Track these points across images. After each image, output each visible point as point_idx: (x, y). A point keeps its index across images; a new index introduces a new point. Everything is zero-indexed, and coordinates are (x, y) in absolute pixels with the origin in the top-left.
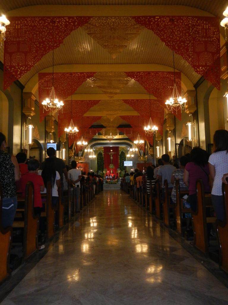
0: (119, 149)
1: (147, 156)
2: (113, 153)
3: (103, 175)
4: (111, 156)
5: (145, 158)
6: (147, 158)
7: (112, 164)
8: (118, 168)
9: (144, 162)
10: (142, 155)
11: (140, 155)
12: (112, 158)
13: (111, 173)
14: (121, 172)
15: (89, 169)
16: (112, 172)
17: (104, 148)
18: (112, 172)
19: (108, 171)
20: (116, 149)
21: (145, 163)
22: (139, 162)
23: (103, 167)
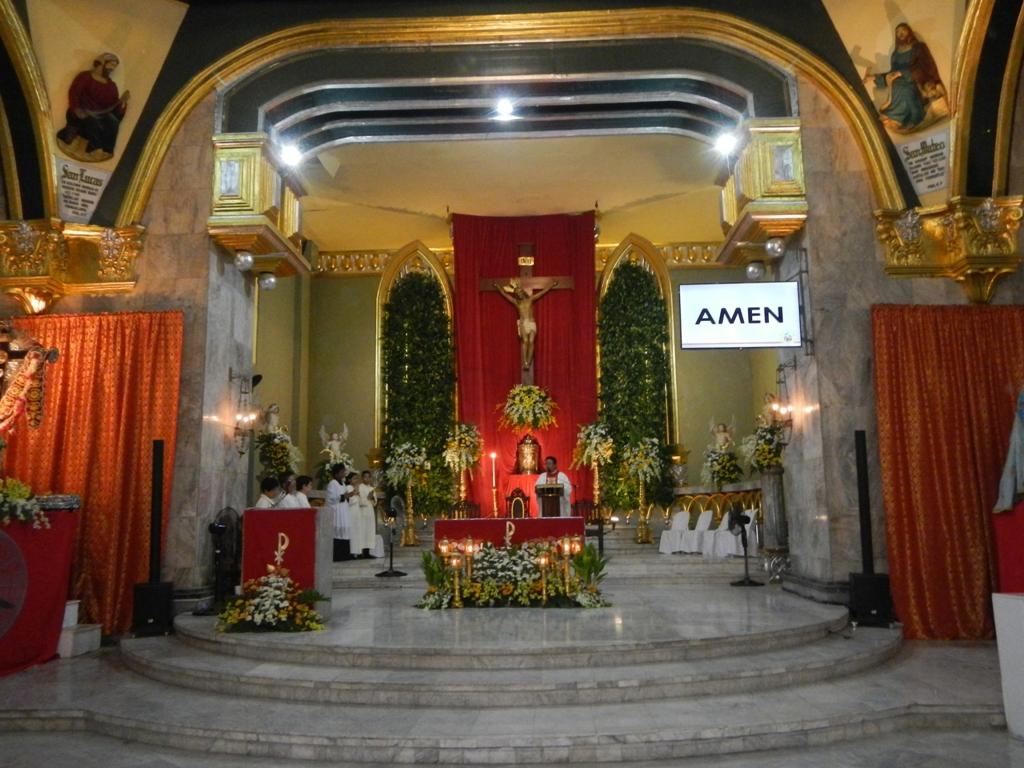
0: (597, 269)
1: (1015, 202)
2: (541, 283)
3: (446, 488)
4: (525, 307)
5: (994, 236)
6: (1018, 234)
7: (535, 384)
8: (590, 418)
9: (962, 298)
10: (937, 191)
11: (900, 204)
12: (528, 326)
13: (518, 470)
14: (616, 457)
15: (190, 387)
16: (528, 461)
17: (465, 228)
18: (528, 461)
19: (490, 446)
20: (566, 237)
21: (980, 304)
22: (893, 293)
23: (446, 408)
